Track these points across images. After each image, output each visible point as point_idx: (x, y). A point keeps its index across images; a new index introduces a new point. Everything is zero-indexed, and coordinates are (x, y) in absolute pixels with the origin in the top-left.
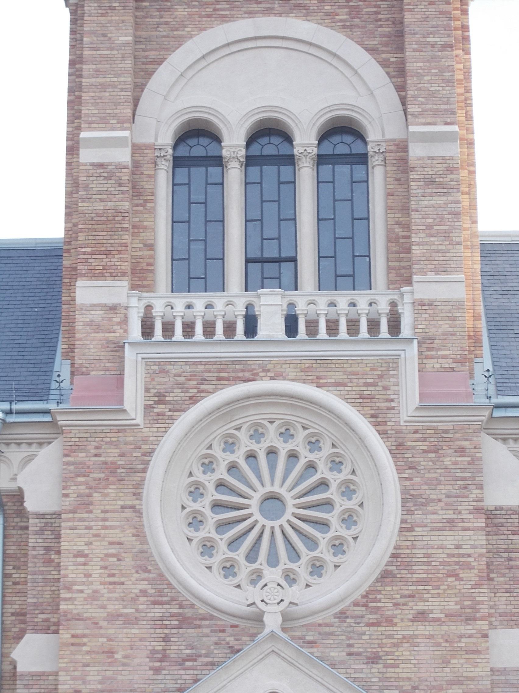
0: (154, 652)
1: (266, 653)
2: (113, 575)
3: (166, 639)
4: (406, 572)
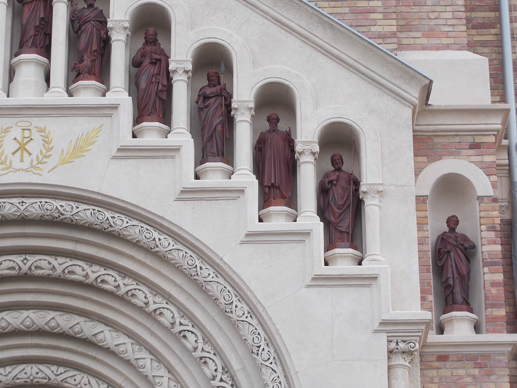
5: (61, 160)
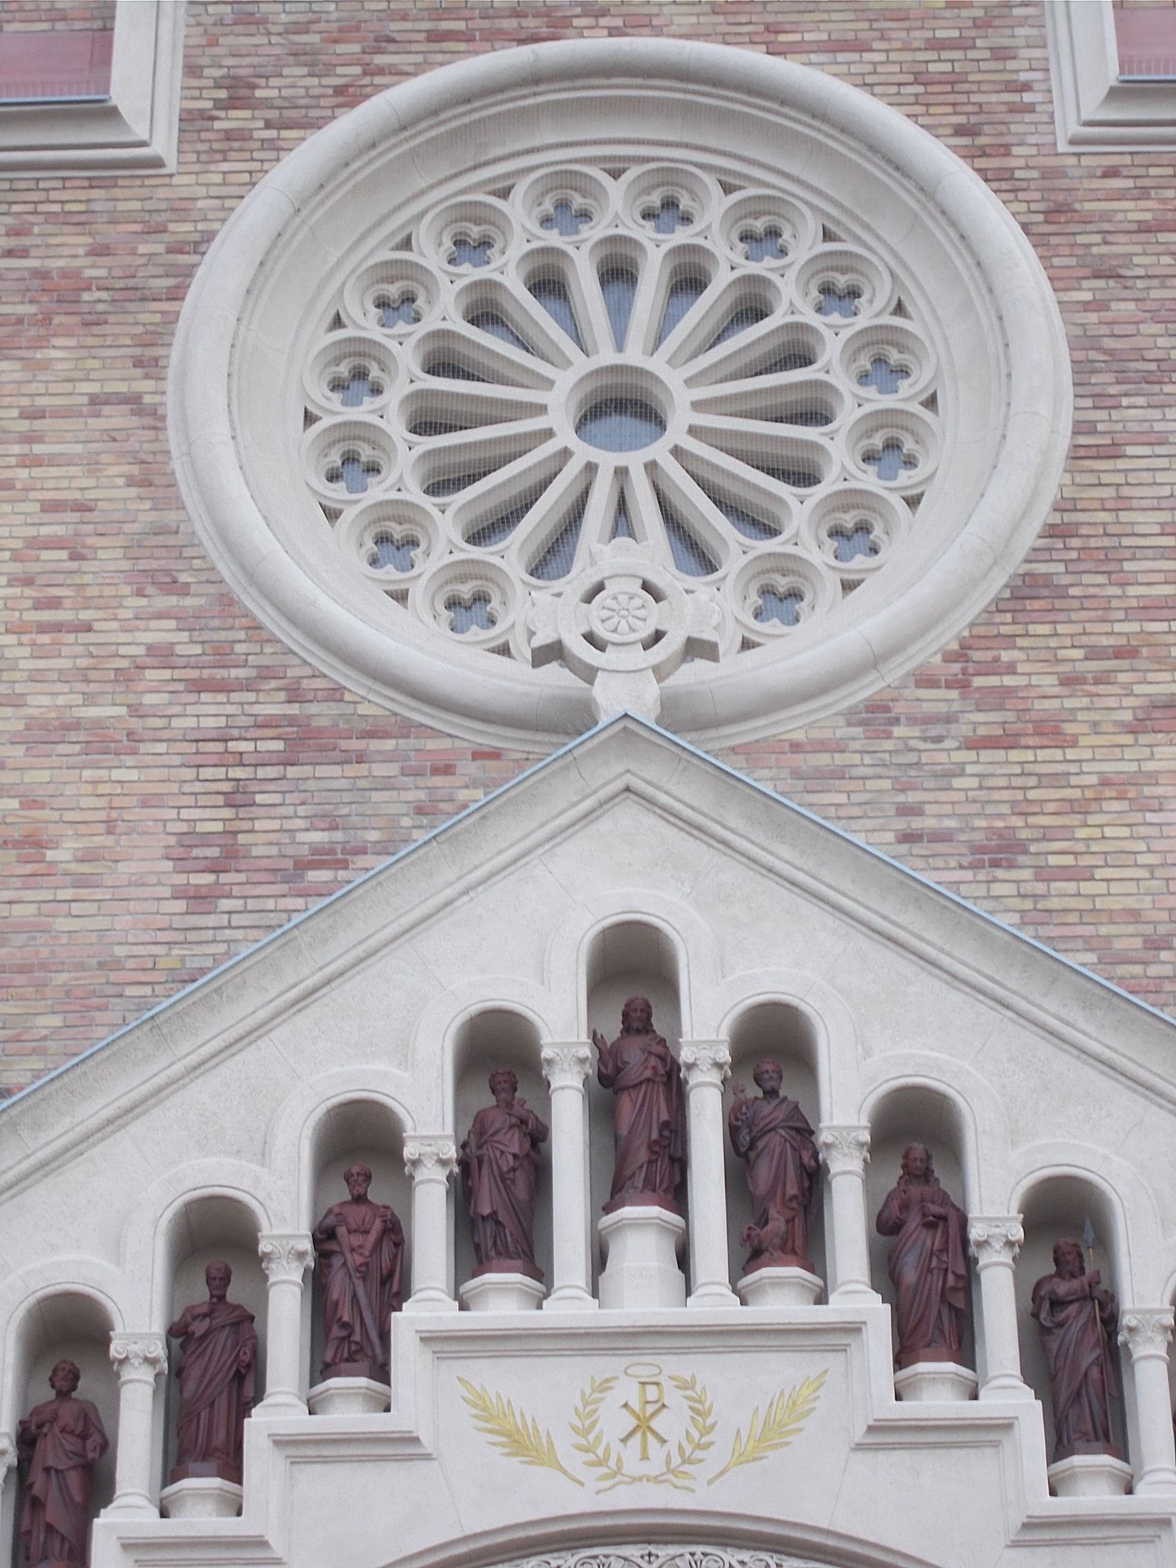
0: (190, 838)
1: (603, 794)
2: (54, 603)
3: (238, 798)
4: (1101, 579)
5: (736, 1454)
